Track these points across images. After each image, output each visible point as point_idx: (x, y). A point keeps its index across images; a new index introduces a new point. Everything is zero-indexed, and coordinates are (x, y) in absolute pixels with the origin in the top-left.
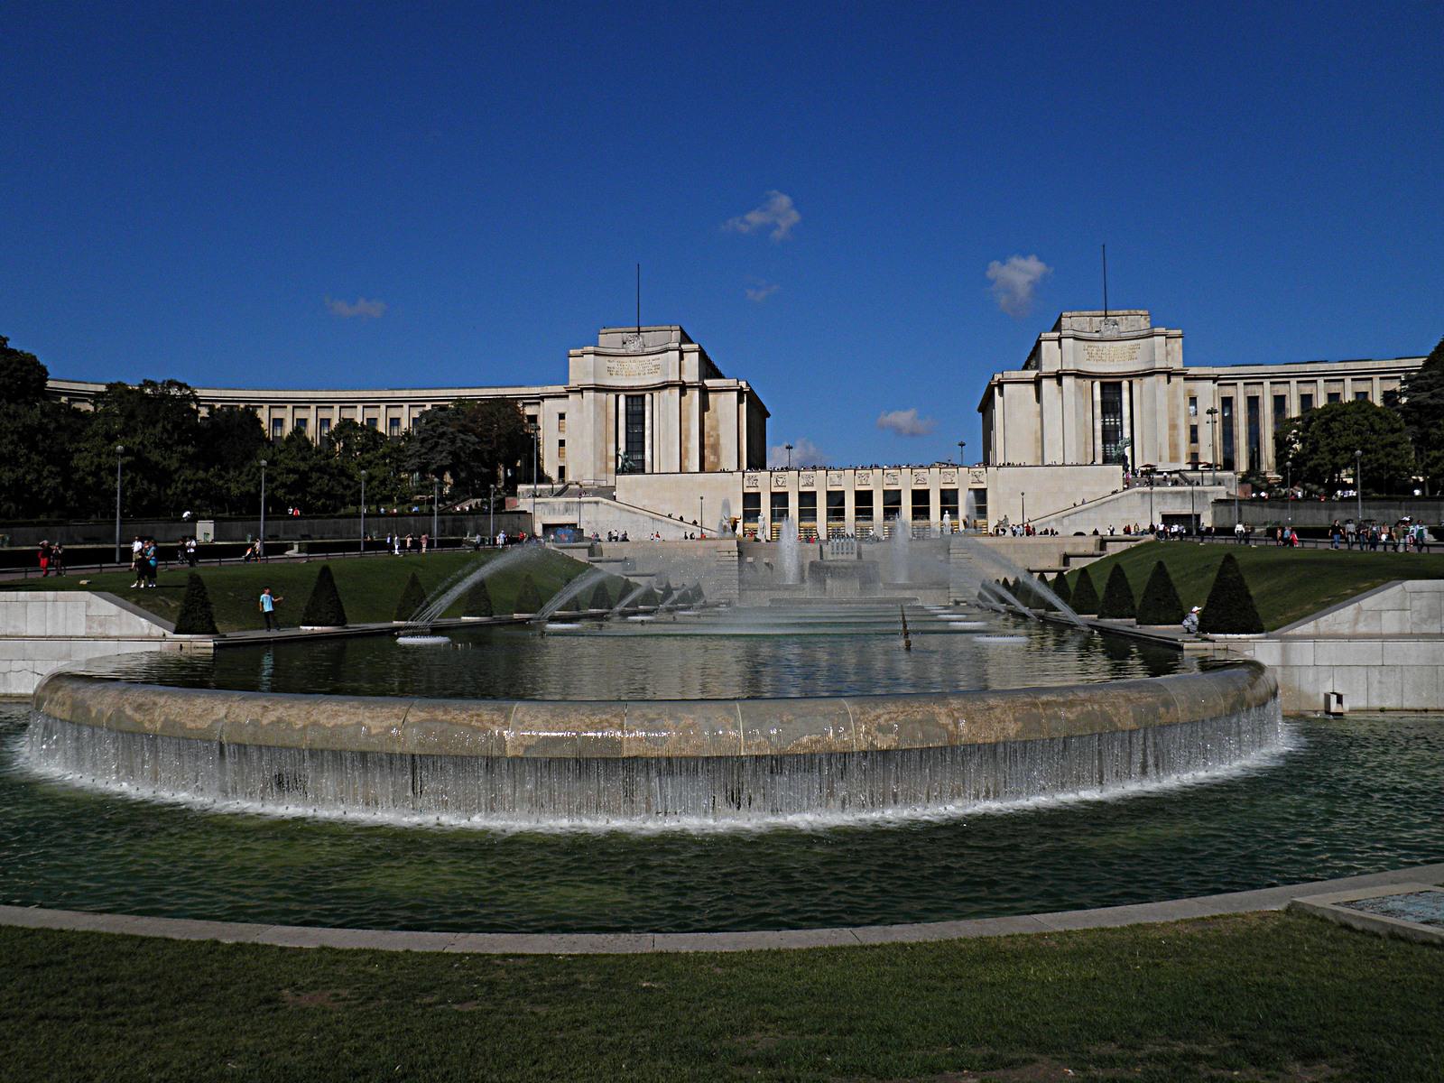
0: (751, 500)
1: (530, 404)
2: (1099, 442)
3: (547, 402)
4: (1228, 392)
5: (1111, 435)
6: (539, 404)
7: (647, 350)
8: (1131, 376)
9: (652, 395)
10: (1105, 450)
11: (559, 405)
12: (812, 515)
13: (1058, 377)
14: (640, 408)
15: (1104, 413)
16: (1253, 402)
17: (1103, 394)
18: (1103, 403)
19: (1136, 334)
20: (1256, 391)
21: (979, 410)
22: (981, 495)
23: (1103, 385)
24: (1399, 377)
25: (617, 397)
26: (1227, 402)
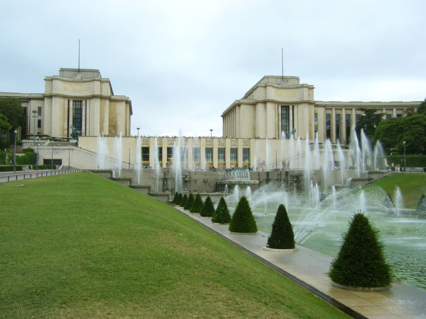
1: (24, 102)
3: (32, 102)
4: (329, 112)
6: (28, 102)
7: (84, 80)
8: (294, 104)
9: (86, 101)
12: (236, 158)
13: (265, 102)
14: (79, 107)
16: (338, 116)
19: (296, 86)
20: (339, 112)
21: (222, 116)
22: (247, 152)
23: (282, 107)
24: (403, 109)
25: (69, 101)
26: (328, 116)
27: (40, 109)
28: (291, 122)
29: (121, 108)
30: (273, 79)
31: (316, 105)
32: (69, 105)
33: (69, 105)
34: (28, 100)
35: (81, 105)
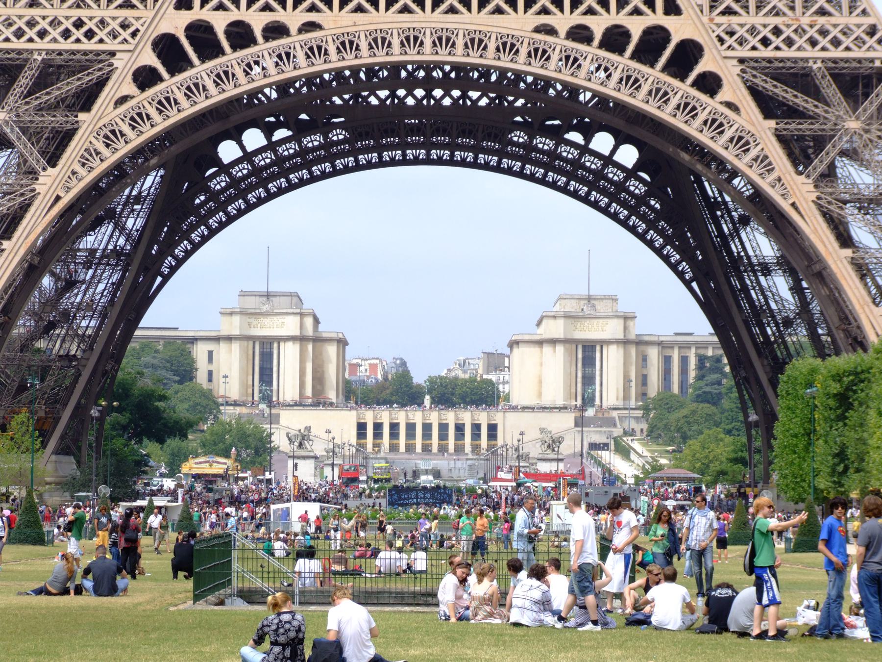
0: (361, 428)
2: (579, 385)
4: (668, 352)
5: (588, 380)
6: (193, 343)
7: (275, 311)
10: (584, 391)
11: (210, 346)
15: (584, 365)
16: (684, 360)
17: (584, 351)
18: (584, 358)
20: (685, 353)
22: (493, 429)
23: (584, 347)
26: (667, 361)
27: (210, 354)
28: (598, 373)
29: (331, 350)
30: (573, 301)
31: (640, 343)
32: (254, 348)
33: (254, 348)
34: (194, 340)
35: (271, 348)
